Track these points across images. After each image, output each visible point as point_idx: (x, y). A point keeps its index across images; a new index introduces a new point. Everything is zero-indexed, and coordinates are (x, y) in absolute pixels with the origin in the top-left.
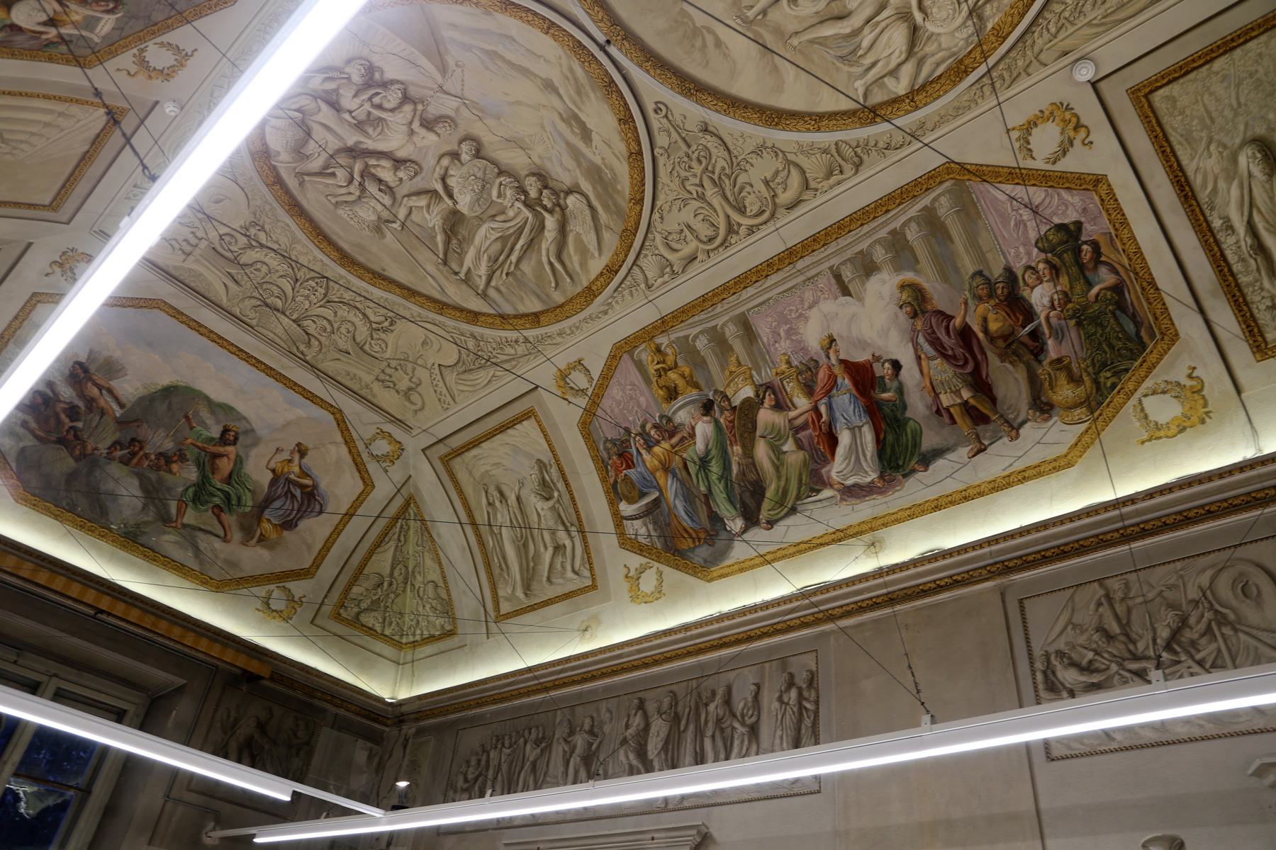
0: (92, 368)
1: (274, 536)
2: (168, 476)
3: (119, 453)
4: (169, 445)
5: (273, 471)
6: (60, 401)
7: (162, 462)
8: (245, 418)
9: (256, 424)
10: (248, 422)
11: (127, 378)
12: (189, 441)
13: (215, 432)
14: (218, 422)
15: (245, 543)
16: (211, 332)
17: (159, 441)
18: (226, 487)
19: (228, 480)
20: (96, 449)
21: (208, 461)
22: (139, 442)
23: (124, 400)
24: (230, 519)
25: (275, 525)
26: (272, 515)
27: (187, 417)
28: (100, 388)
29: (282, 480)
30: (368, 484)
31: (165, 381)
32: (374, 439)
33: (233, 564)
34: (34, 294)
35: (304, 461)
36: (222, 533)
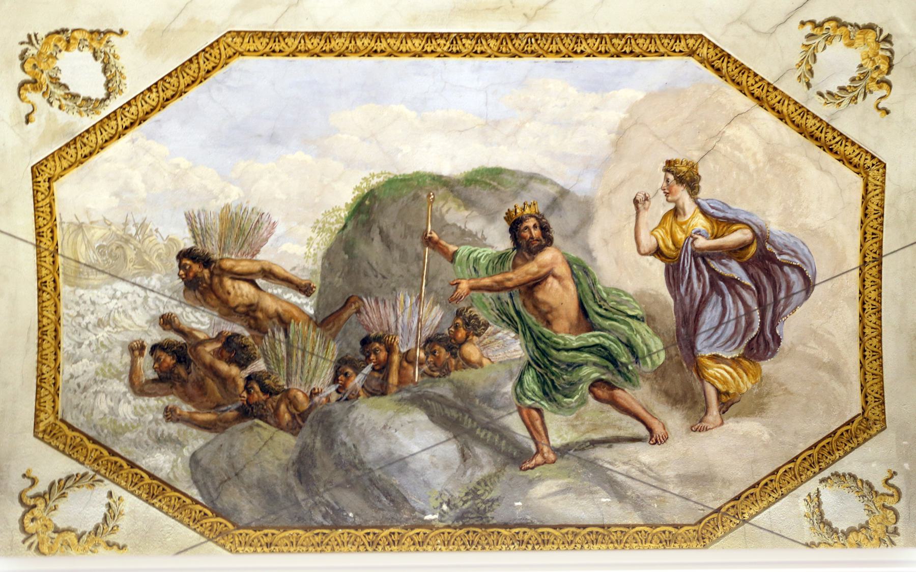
0: (213, 248)
1: (746, 384)
2: (468, 375)
3: (357, 381)
4: (434, 317)
5: (658, 252)
6: (202, 342)
7: (443, 353)
8: (532, 177)
9: (564, 175)
10: (544, 181)
11: (279, 230)
12: (464, 286)
13: (499, 240)
14: (490, 217)
15: (698, 427)
16: (354, 36)
17: (411, 318)
18: (590, 338)
19: (584, 320)
20: (313, 394)
21: (524, 304)
22: (378, 339)
23: (303, 277)
24: (639, 395)
25: (735, 362)
26: (715, 340)
27: (428, 241)
28: (248, 278)
29: (688, 263)
30: (866, 165)
31: (345, 196)
32: (810, 56)
33: (702, 479)
34: (36, 171)
35: (702, 195)
36: (642, 431)
